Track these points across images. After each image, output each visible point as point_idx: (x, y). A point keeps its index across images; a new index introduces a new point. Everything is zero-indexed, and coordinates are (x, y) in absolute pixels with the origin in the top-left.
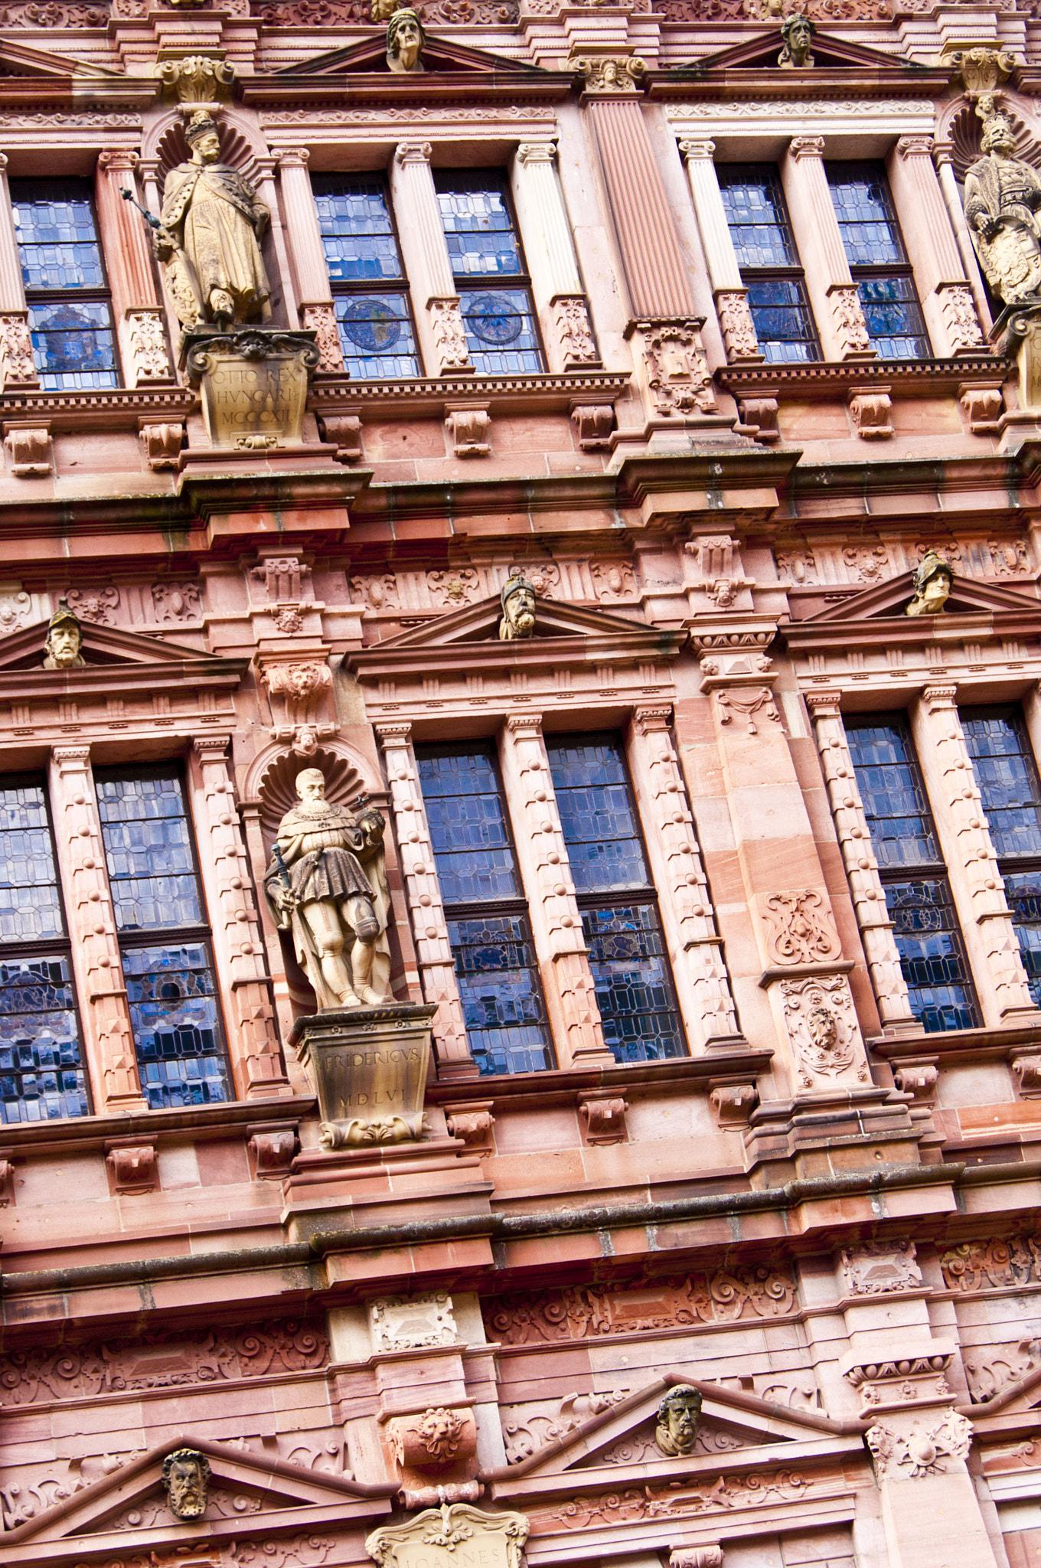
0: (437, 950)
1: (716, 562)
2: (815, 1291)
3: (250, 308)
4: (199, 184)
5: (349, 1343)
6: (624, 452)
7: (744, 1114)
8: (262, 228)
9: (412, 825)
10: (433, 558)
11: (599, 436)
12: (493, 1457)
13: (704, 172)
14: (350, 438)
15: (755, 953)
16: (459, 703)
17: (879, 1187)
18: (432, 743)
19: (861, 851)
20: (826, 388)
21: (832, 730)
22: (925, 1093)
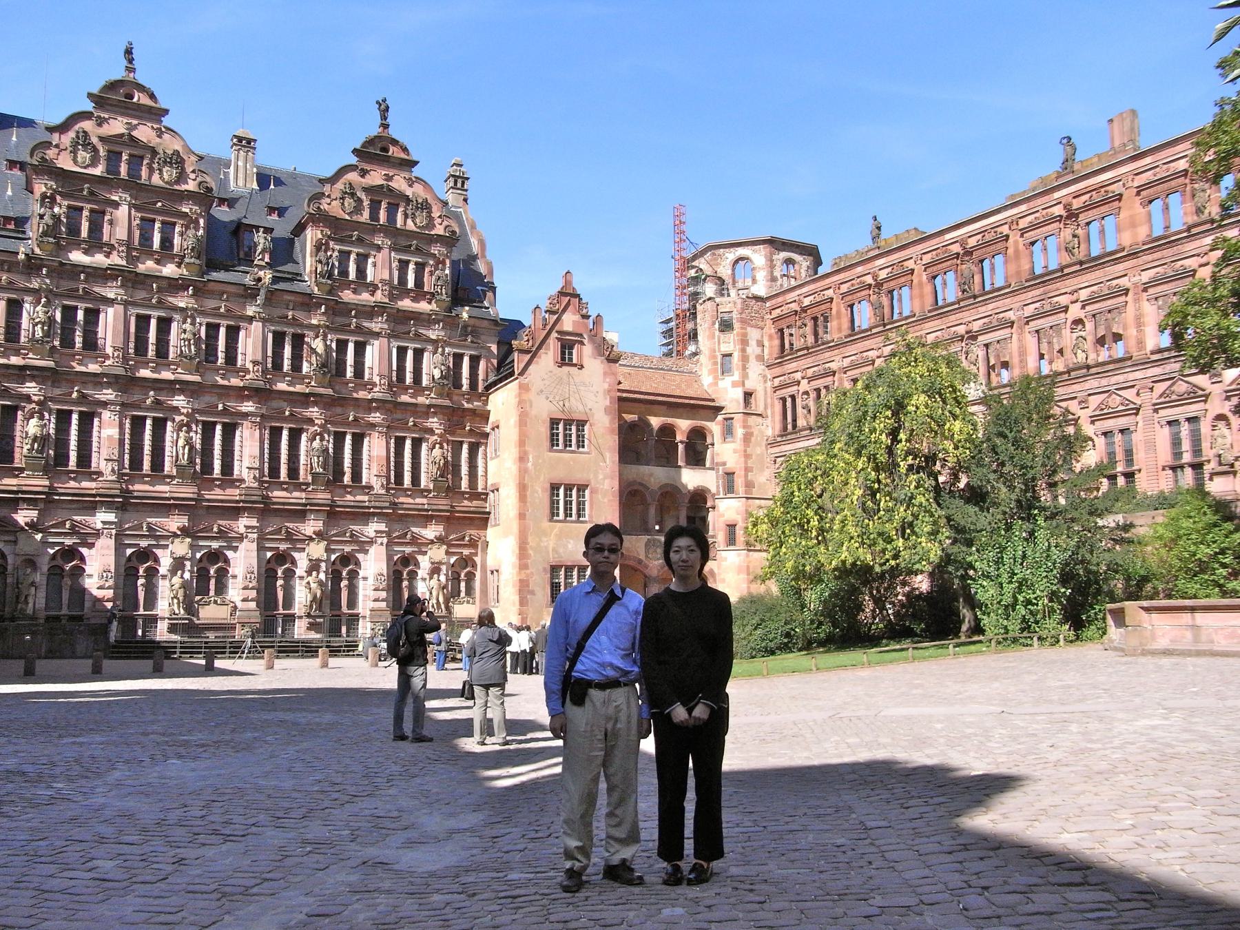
15: (374, 471)
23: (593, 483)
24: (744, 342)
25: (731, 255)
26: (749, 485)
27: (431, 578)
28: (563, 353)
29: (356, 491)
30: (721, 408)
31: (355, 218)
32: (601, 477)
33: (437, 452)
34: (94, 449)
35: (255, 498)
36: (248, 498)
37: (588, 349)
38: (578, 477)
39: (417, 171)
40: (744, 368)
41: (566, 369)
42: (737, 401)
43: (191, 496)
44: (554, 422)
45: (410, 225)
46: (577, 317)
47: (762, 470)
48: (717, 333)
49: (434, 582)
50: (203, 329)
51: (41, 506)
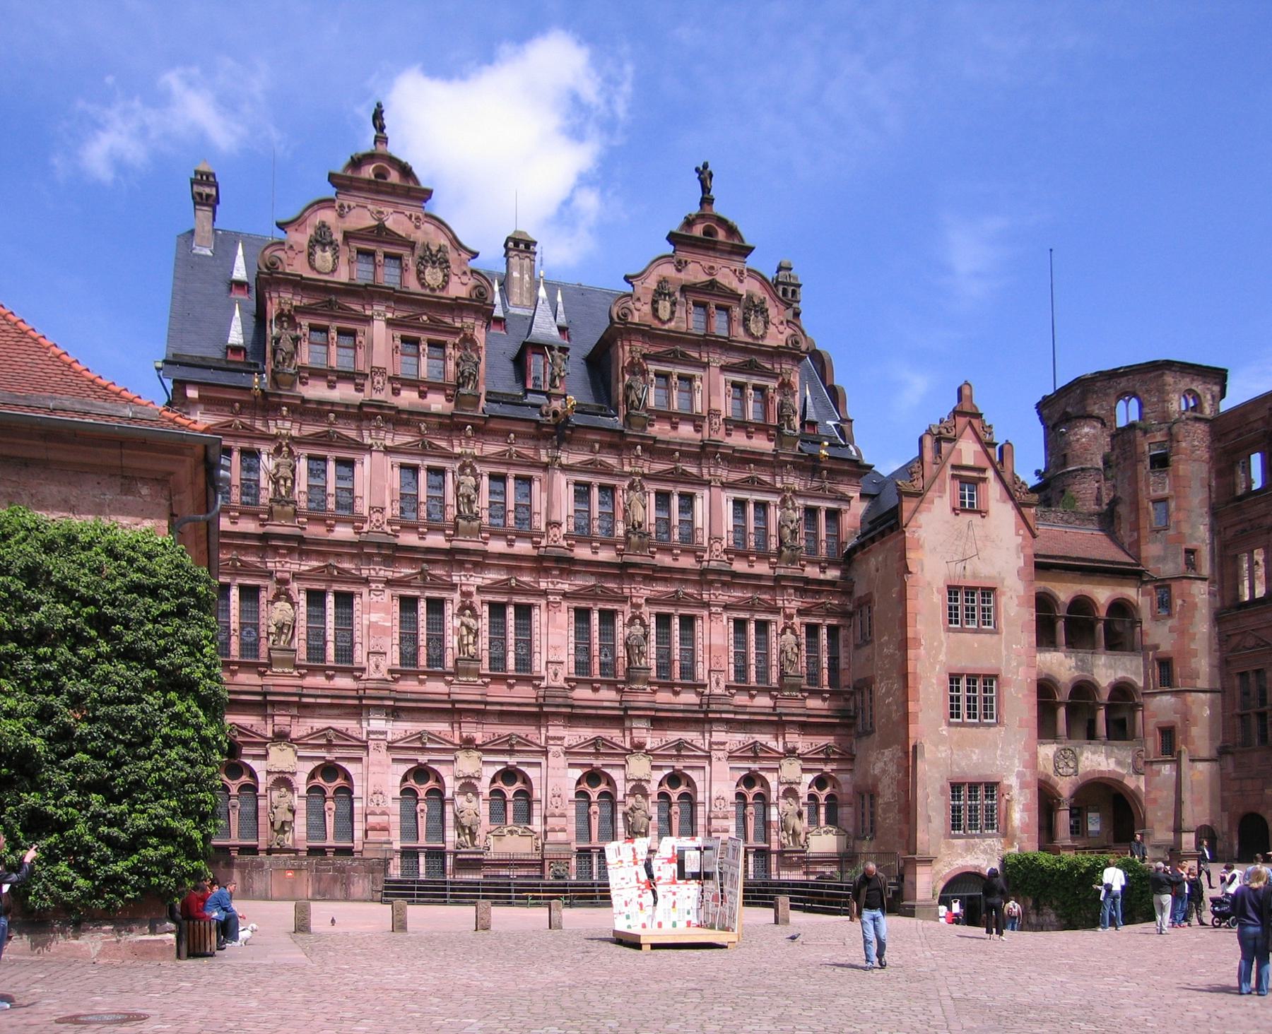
0: (654, 656)
1: (717, 589)
2: (707, 727)
4: (635, 496)
5: (627, 724)
6: (705, 564)
7: (702, 694)
9: (653, 631)
10: (665, 580)
11: (699, 560)
12: (648, 747)
13: (731, 504)
14: (653, 553)
16: (665, 610)
17: (721, 712)
18: (659, 617)
19: (732, 648)
20: (744, 555)
21: (732, 624)
22: (733, 695)
28: (963, 497)
31: (672, 325)
34: (357, 640)
35: (560, 701)
36: (549, 701)
37: (993, 489)
39: (751, 261)
43: (479, 698)
44: (953, 590)
50: (485, 482)
51: (295, 712)
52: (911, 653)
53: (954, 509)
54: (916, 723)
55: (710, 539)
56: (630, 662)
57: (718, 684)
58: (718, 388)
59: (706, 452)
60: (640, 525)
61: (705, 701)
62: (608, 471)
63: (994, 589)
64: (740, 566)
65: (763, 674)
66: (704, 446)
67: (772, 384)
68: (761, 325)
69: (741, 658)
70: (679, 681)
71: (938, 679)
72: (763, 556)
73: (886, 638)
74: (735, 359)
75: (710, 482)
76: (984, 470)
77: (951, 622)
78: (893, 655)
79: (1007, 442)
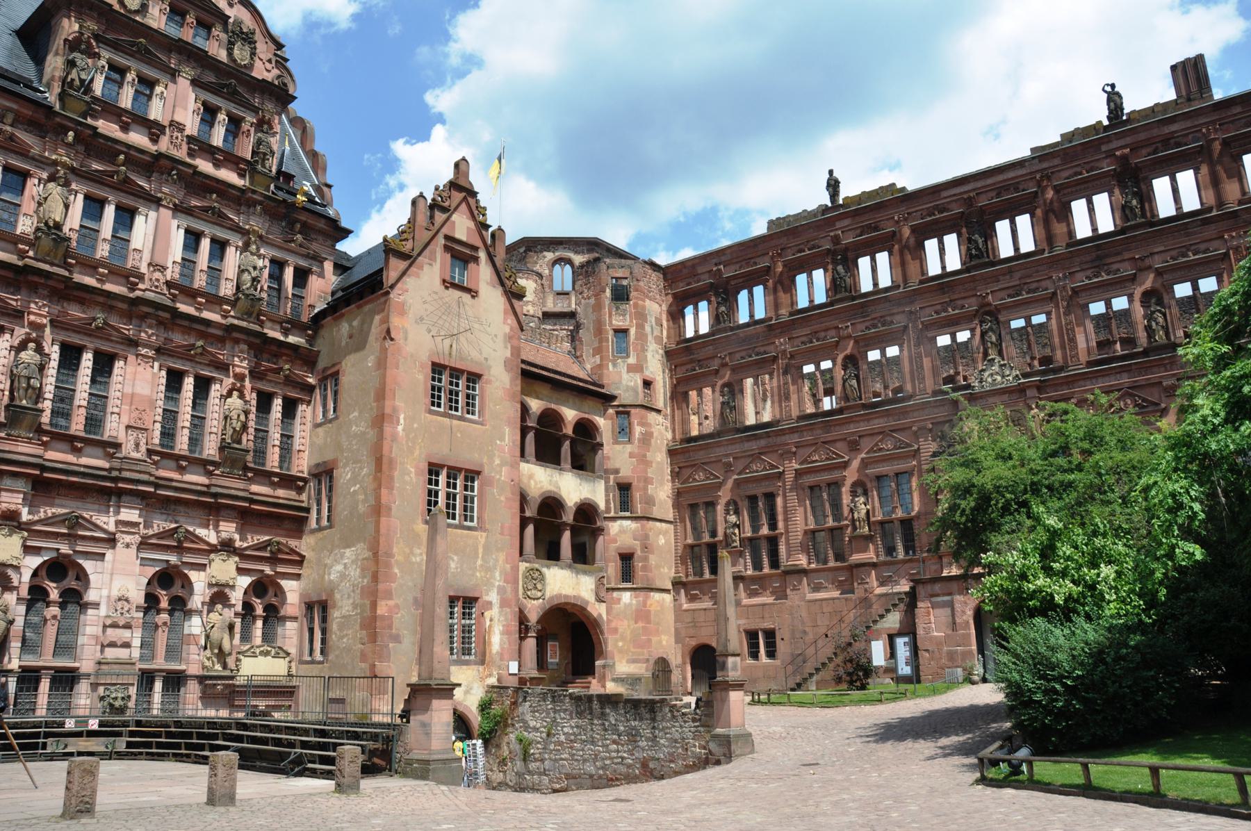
0: (49, 396)
3: (58, 226)
8: (67, 207)
9: (54, 364)
10: (82, 302)
13: (182, 232)
15: (125, 420)
16: (76, 339)
19: (160, 403)
20: (192, 294)
21: (164, 373)
23: (486, 471)
24: (641, 316)
25: (550, 256)
26: (650, 501)
27: (209, 612)
29: (88, 450)
30: (613, 398)
32: (497, 462)
33: (235, 401)
38: (466, 458)
40: (644, 350)
41: (456, 294)
42: (635, 390)
44: (437, 368)
45: (223, 55)
46: (471, 224)
47: (662, 484)
48: (607, 302)
49: (214, 617)
52: (387, 429)
53: (444, 281)
54: (389, 515)
55: (150, 264)
56: (12, 397)
57: (137, 445)
58: (186, 98)
59: (157, 164)
60: (58, 226)
61: (116, 464)
62: (24, 154)
63: (479, 376)
64: (183, 308)
65: (195, 441)
66: (160, 156)
67: (250, 119)
68: (247, 54)
69: (170, 416)
70: (83, 434)
71: (417, 467)
72: (215, 300)
73: (356, 414)
74: (210, 78)
75: (160, 199)
76: (476, 249)
77: (433, 404)
78: (364, 433)
79: (500, 229)
